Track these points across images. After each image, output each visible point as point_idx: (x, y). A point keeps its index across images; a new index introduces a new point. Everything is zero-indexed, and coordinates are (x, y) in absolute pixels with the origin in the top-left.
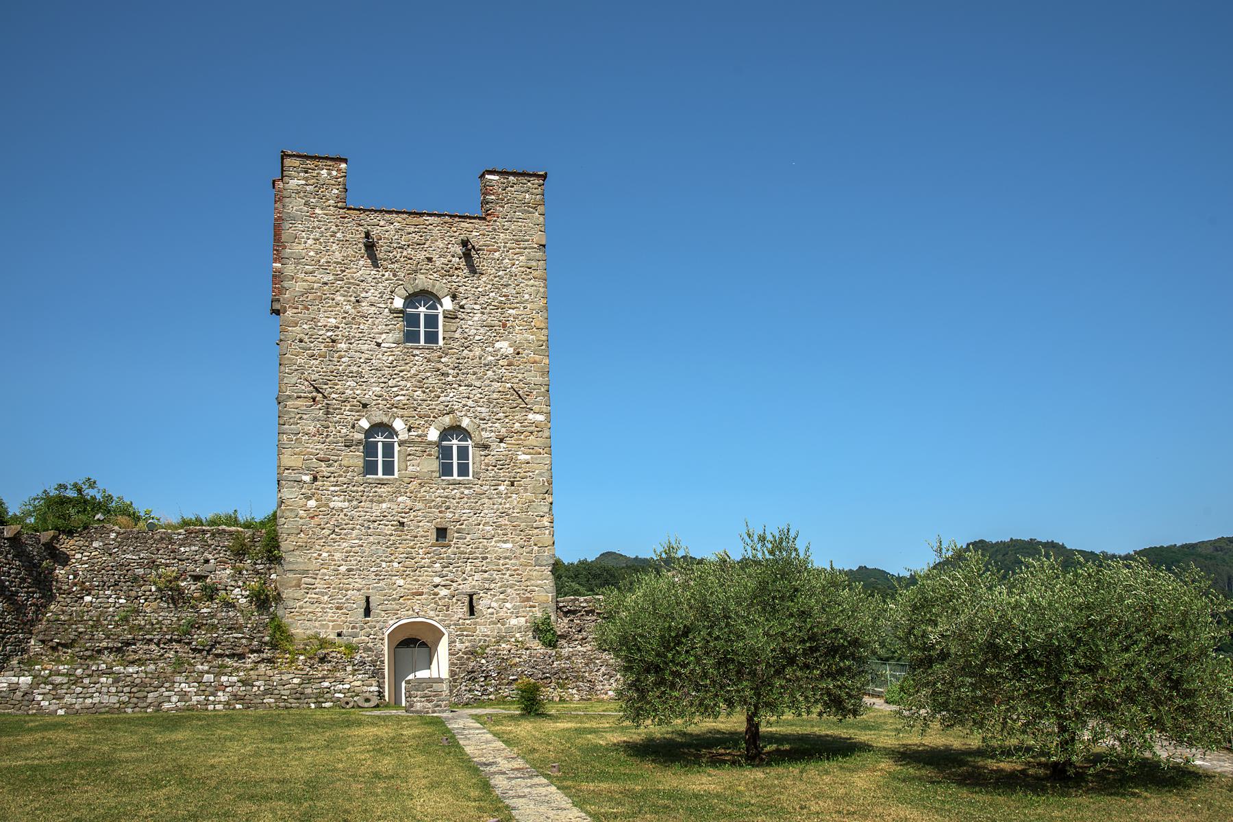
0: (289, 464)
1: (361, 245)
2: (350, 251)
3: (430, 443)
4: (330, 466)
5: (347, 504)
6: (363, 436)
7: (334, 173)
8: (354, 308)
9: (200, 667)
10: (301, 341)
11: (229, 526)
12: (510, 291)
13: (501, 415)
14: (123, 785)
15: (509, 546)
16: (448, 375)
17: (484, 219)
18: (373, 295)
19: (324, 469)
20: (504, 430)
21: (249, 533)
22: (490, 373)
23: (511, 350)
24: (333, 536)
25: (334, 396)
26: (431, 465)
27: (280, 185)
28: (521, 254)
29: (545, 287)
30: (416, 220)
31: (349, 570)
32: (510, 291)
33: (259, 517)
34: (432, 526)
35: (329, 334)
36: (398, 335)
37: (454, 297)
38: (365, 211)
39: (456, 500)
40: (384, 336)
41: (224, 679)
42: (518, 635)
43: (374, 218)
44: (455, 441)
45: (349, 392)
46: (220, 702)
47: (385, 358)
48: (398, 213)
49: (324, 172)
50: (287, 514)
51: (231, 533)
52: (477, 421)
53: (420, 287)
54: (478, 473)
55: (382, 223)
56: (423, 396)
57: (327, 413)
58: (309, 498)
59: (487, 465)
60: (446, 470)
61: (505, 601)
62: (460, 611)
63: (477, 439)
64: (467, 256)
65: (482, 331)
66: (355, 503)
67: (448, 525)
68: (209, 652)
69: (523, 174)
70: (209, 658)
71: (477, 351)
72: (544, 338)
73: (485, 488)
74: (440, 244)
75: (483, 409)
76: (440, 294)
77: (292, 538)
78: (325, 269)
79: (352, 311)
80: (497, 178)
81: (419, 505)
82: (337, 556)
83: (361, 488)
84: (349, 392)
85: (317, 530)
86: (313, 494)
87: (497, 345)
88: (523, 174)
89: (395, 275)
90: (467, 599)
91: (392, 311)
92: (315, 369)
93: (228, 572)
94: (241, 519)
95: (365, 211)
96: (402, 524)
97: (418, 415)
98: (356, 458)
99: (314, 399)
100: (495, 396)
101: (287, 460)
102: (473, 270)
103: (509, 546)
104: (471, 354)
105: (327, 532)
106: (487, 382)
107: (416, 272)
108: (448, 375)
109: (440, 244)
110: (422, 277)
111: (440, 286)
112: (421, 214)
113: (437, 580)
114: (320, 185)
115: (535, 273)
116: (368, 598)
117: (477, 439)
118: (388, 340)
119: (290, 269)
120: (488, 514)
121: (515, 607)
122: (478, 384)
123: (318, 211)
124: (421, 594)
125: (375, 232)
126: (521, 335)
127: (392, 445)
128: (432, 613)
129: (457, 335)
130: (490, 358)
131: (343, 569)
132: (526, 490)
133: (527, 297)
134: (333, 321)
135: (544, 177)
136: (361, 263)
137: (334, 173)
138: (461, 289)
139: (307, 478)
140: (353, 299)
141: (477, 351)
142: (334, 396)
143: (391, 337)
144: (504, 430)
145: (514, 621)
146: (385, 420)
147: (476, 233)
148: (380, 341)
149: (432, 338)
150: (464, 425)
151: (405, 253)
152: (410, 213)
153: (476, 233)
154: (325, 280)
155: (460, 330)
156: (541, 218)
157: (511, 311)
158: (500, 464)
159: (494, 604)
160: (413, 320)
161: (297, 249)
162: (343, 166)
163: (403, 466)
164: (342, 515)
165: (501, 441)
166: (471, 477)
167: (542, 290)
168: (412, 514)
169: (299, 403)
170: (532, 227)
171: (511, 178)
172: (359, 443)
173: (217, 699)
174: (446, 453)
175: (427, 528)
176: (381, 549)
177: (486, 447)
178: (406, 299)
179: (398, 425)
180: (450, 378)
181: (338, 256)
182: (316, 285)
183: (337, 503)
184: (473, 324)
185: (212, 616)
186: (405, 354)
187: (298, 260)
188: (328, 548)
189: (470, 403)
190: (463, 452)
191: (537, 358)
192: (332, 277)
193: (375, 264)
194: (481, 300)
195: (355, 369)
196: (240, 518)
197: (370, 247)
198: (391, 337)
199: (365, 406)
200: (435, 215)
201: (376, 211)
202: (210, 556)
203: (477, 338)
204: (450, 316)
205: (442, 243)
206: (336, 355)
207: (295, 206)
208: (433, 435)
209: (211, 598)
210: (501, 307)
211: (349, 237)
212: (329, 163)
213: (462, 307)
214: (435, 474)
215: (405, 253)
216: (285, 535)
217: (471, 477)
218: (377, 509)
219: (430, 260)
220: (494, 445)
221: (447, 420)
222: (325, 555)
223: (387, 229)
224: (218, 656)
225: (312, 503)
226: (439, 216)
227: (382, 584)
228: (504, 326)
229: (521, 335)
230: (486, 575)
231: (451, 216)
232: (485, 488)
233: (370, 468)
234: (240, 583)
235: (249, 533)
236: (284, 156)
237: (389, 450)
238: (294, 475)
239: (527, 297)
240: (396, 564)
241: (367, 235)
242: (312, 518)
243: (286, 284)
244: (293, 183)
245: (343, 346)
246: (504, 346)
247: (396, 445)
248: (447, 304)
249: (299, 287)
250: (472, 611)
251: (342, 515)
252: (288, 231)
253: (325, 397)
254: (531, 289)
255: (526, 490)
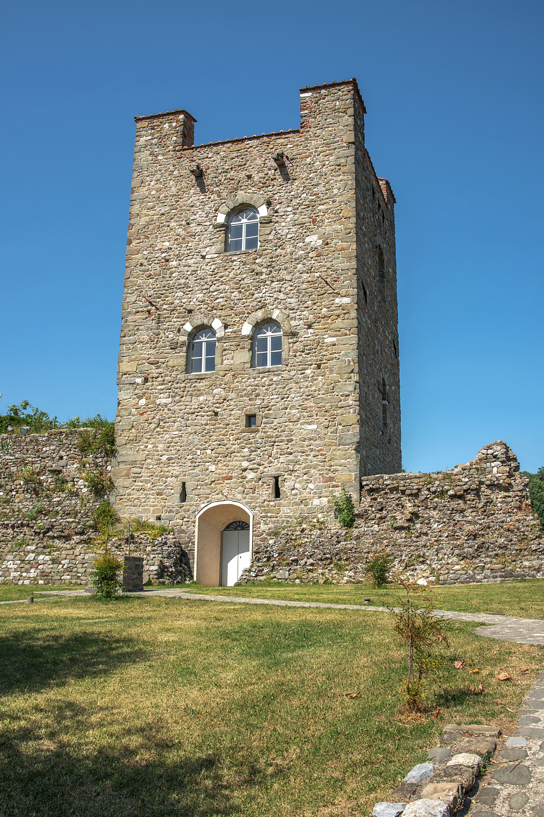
3: (244, 337)
4: (158, 367)
5: (170, 400)
7: (174, 124)
8: (185, 230)
10: (142, 265)
15: (314, 427)
16: (261, 274)
17: (298, 131)
18: (200, 216)
19: (154, 371)
22: (299, 266)
23: (320, 242)
26: (243, 356)
28: (331, 155)
31: (169, 459)
35: (163, 255)
36: (220, 246)
37: (269, 204)
39: (266, 388)
42: (320, 516)
53: (240, 201)
55: (210, 155)
58: (140, 398)
59: (296, 351)
61: (308, 482)
62: (266, 492)
65: (294, 229)
66: (177, 398)
67: (257, 411)
69: (333, 85)
71: (289, 248)
73: (293, 373)
75: (293, 300)
77: (125, 433)
80: (310, 94)
81: (232, 395)
82: (161, 446)
83: (183, 385)
86: (144, 394)
87: (307, 240)
88: (333, 85)
89: (219, 196)
90: (273, 481)
91: (216, 227)
93: (75, 466)
96: (216, 414)
97: (232, 313)
98: (178, 359)
99: (149, 311)
100: (304, 286)
101: (125, 367)
103: (314, 427)
106: (297, 275)
107: (236, 189)
110: (242, 192)
112: (243, 140)
113: (245, 464)
115: (343, 169)
116: (184, 484)
118: (211, 252)
120: (295, 398)
121: (317, 487)
122: (288, 277)
124: (230, 478)
126: (329, 228)
128: (239, 496)
129: (271, 237)
131: (164, 458)
132: (331, 371)
134: (167, 244)
136: (192, 191)
138: (276, 197)
139: (139, 380)
140: (184, 223)
143: (213, 249)
144: (311, 316)
145: (316, 502)
146: (206, 321)
147: (288, 146)
148: (204, 254)
150: (274, 317)
152: (233, 142)
154: (163, 211)
155: (274, 232)
159: (298, 486)
161: (143, 191)
164: (166, 411)
165: (310, 327)
168: (226, 403)
169: (138, 316)
171: (323, 91)
172: (183, 344)
175: (235, 415)
177: (294, 334)
179: (217, 324)
180: (264, 277)
183: (163, 400)
184: (284, 227)
189: (281, 296)
193: (203, 190)
198: (213, 249)
199: (190, 311)
200: (254, 138)
201: (205, 146)
203: (289, 236)
204: (267, 221)
205: (259, 158)
206: (168, 272)
208: (247, 329)
210: (311, 206)
212: (171, 117)
213: (276, 212)
220: (301, 333)
221: (260, 315)
222: (150, 446)
224: (54, 537)
225: (143, 402)
226: (258, 138)
227: (197, 470)
228: (314, 221)
230: (291, 457)
231: (268, 136)
232: (293, 373)
238: (130, 379)
239: (335, 191)
240: (209, 452)
245: (174, 263)
246: (314, 240)
248: (263, 211)
249: (143, 220)
250: (277, 494)
251: (166, 411)
253: (157, 309)
255: (331, 371)
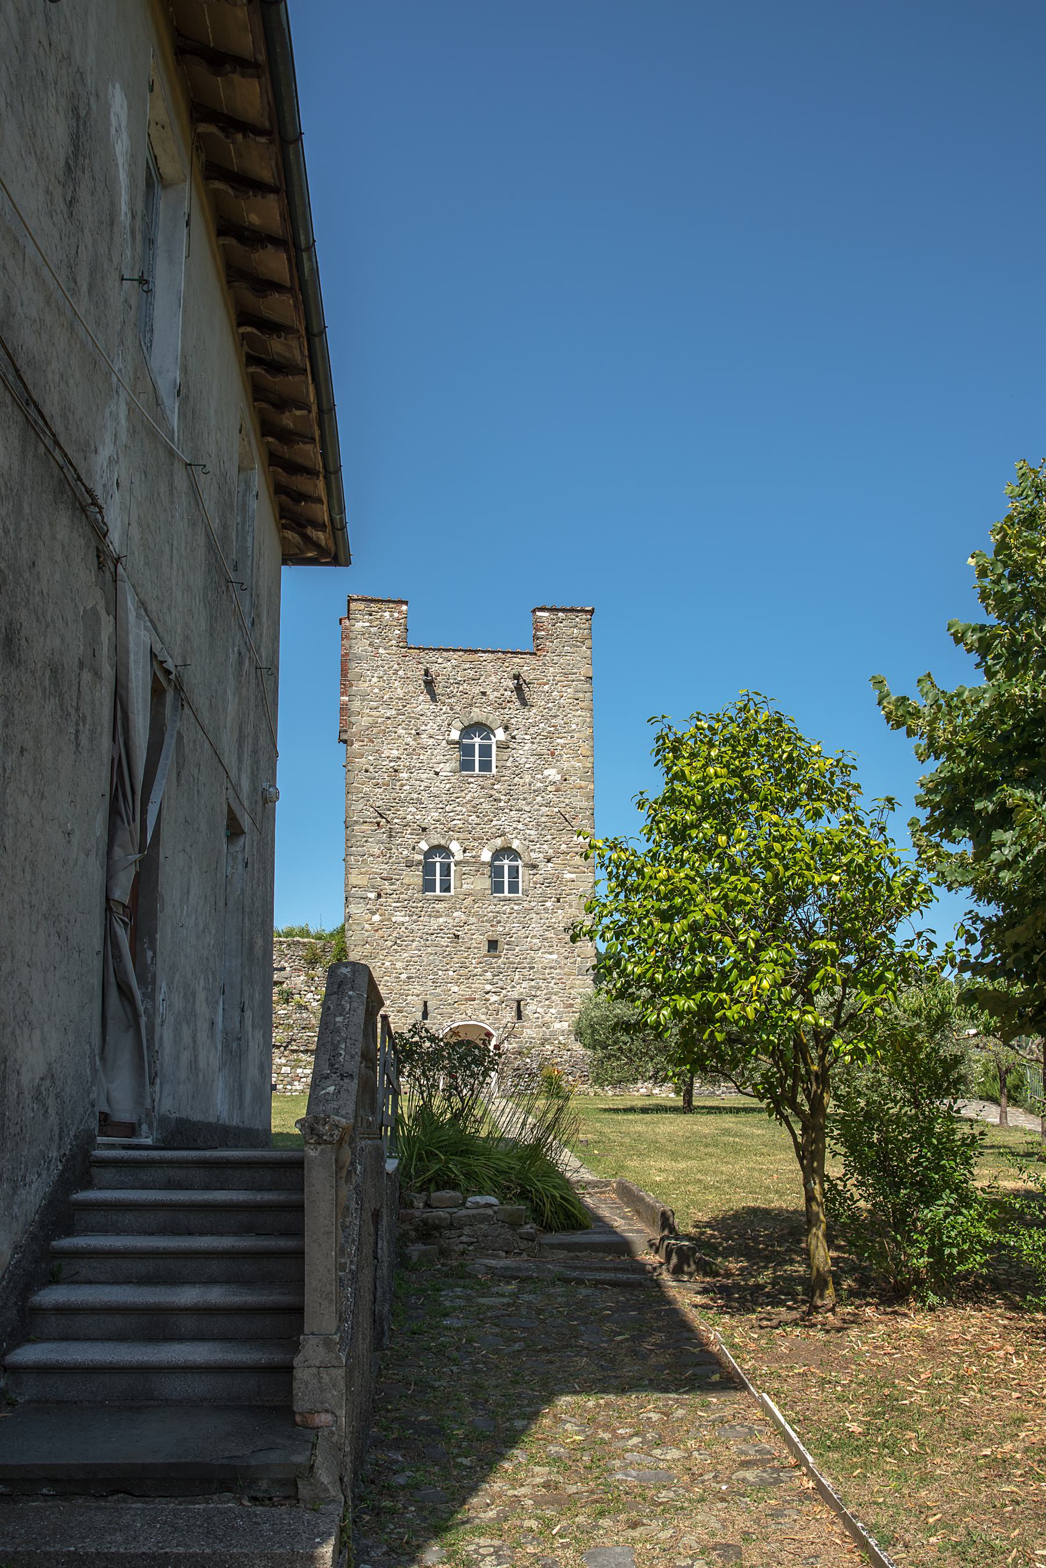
0: (355, 883)
1: (421, 682)
2: (411, 688)
3: (483, 863)
4: (392, 884)
5: (407, 918)
6: (422, 857)
7: (396, 615)
8: (415, 740)
9: (279, 1061)
10: (367, 771)
11: (302, 937)
12: (559, 721)
13: (549, 837)
14: (381, 1206)
15: (555, 957)
16: (500, 800)
17: (535, 654)
18: (431, 728)
19: (387, 887)
20: (551, 851)
21: (321, 943)
22: (539, 799)
23: (559, 777)
24: (395, 947)
25: (396, 821)
26: (484, 883)
27: (347, 622)
28: (569, 686)
29: (592, 717)
30: (472, 657)
31: (409, 978)
32: (559, 721)
33: (329, 928)
34: (484, 938)
35: (392, 764)
36: (454, 765)
37: (506, 728)
38: (424, 649)
39: (507, 915)
40: (442, 765)
41: (299, 1071)
42: (561, 1038)
43: (432, 656)
44: (506, 861)
45: (409, 817)
46: (296, 1090)
47: (442, 786)
48: (454, 650)
49: (387, 614)
50: (355, 927)
51: (304, 944)
52: (527, 843)
53: (475, 720)
54: (527, 890)
55: (440, 660)
56: (478, 820)
57: (390, 836)
58: (374, 913)
59: (535, 883)
60: (498, 888)
61: (549, 1007)
62: (508, 1016)
63: (526, 859)
64: (518, 689)
65: (532, 759)
66: (415, 917)
67: (498, 937)
68: (285, 1048)
69: (572, 610)
70: (286, 1053)
71: (527, 778)
72: (590, 765)
73: (533, 904)
74: (493, 679)
75: (532, 832)
76: (493, 726)
77: (359, 949)
78: (388, 704)
79: (412, 743)
80: (546, 614)
81: (472, 920)
82: (399, 965)
83: (420, 904)
84: (409, 817)
85: (381, 941)
86: (378, 910)
87: (546, 773)
88: (572, 610)
89: (452, 709)
90: (515, 1005)
91: (449, 743)
92: (380, 797)
93: (302, 978)
94: (313, 931)
95: (424, 649)
96: (457, 937)
97: (473, 838)
98: (415, 877)
99: (378, 824)
100: (543, 819)
101: (354, 879)
102: (524, 703)
103: (555, 957)
104: (522, 781)
105: (389, 943)
106: (536, 807)
107: (471, 705)
108: (500, 800)
109: (493, 679)
110: (477, 710)
111: (493, 718)
112: (476, 652)
113: (488, 987)
114: (383, 627)
115: (582, 704)
116: (425, 1003)
117: (526, 859)
118: (445, 769)
119: (356, 706)
120: (536, 928)
121: (559, 1013)
122: (528, 809)
123: (381, 651)
124: (474, 1000)
125: (434, 669)
126: (568, 763)
127: (449, 865)
128: (483, 1017)
129: (509, 764)
130: (539, 785)
131: (404, 977)
132: (571, 906)
133: (574, 726)
134: (395, 753)
135: (592, 612)
136: (421, 698)
137: (396, 615)
138: (512, 721)
139: (372, 895)
140: (413, 732)
141: (527, 778)
142: (396, 821)
143: (448, 767)
144: (551, 851)
145: (557, 1026)
146: (443, 842)
147: (527, 668)
148: (438, 770)
149: (486, 766)
150: (514, 847)
151: (461, 688)
152: (465, 651)
153: (527, 668)
154: (388, 715)
155: (511, 759)
156: (589, 652)
157: (559, 741)
158: (547, 882)
159: (539, 1010)
160: (468, 750)
161: (363, 686)
162: (404, 608)
163: (458, 885)
164: (403, 929)
165: (549, 861)
166: (520, 894)
167: (588, 720)
168: (467, 927)
169: (364, 827)
170: (578, 660)
171: (560, 614)
172: (419, 863)
173: (294, 1088)
174: (498, 872)
175: (479, 941)
176: (438, 959)
177: (534, 867)
178: (462, 731)
179: (455, 847)
180: (502, 804)
181: (400, 692)
182: (380, 720)
183: (399, 917)
184: (523, 753)
185: (288, 1016)
186: (461, 782)
187: (364, 697)
188: (391, 958)
189: (520, 826)
190: (514, 872)
191: (583, 783)
192: (394, 712)
193: (434, 699)
194: (532, 731)
195: (415, 796)
196: (312, 930)
197: (429, 684)
198: (448, 767)
199: (424, 830)
200: (489, 652)
201: (434, 650)
202: (286, 965)
203: (527, 766)
204: (503, 746)
205: (496, 679)
206: (398, 784)
207: (360, 647)
208: (486, 856)
209: (287, 1002)
210: (550, 736)
211: (409, 674)
212: (391, 605)
213: (514, 737)
214: (487, 892)
215: (461, 688)
216: (352, 947)
217: (520, 894)
218: (435, 923)
219: (484, 694)
220: (542, 865)
221: (499, 842)
222: (387, 964)
223: (444, 666)
224: (296, 1051)
225: (376, 918)
226: (493, 652)
227: (438, 990)
228: (553, 754)
229: (568, 763)
230: (533, 983)
231: (503, 653)
232: (533, 904)
233: (428, 886)
234: (313, 989)
235: (321, 943)
236: (350, 600)
237: (446, 870)
238: (360, 893)
239: (574, 726)
240: (451, 973)
241: (427, 673)
242: (377, 931)
243: (353, 719)
244: (359, 625)
245: (404, 775)
246: (552, 774)
247: (452, 865)
248: (500, 735)
249: (365, 721)
250: (519, 1015)
251: (403, 929)
252: (355, 669)
253: (388, 822)
254: (578, 719)
255: (571, 906)
